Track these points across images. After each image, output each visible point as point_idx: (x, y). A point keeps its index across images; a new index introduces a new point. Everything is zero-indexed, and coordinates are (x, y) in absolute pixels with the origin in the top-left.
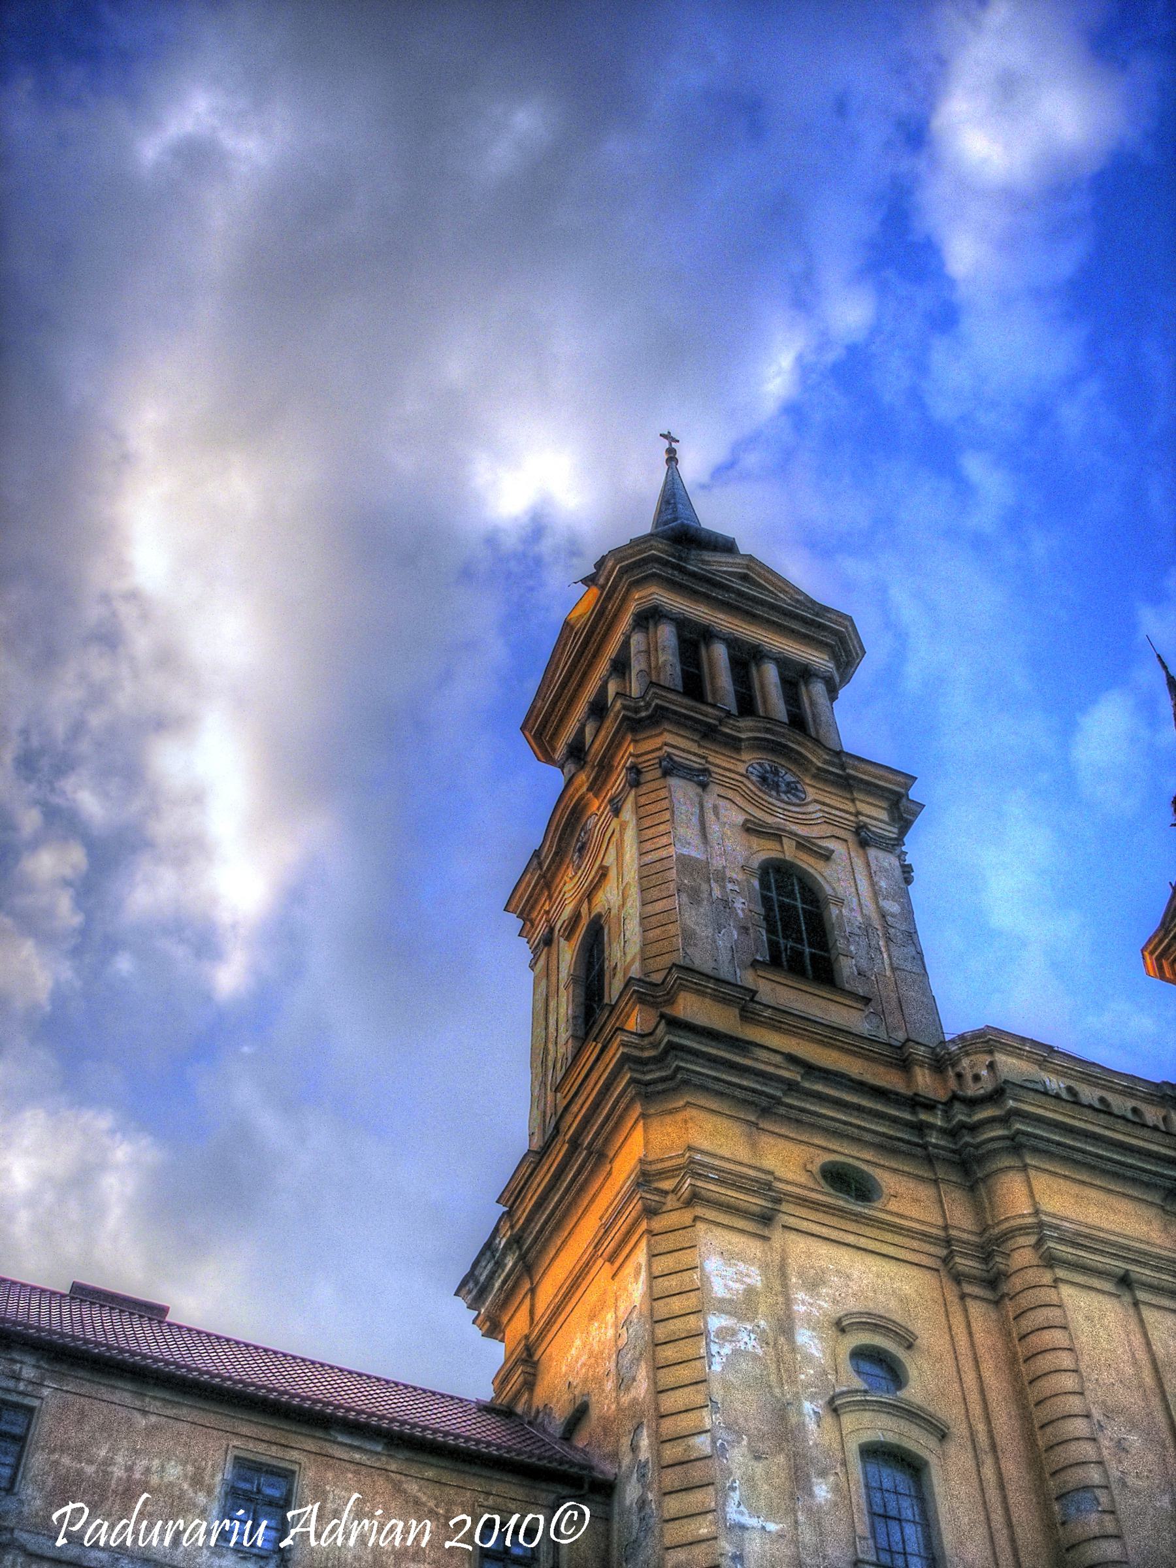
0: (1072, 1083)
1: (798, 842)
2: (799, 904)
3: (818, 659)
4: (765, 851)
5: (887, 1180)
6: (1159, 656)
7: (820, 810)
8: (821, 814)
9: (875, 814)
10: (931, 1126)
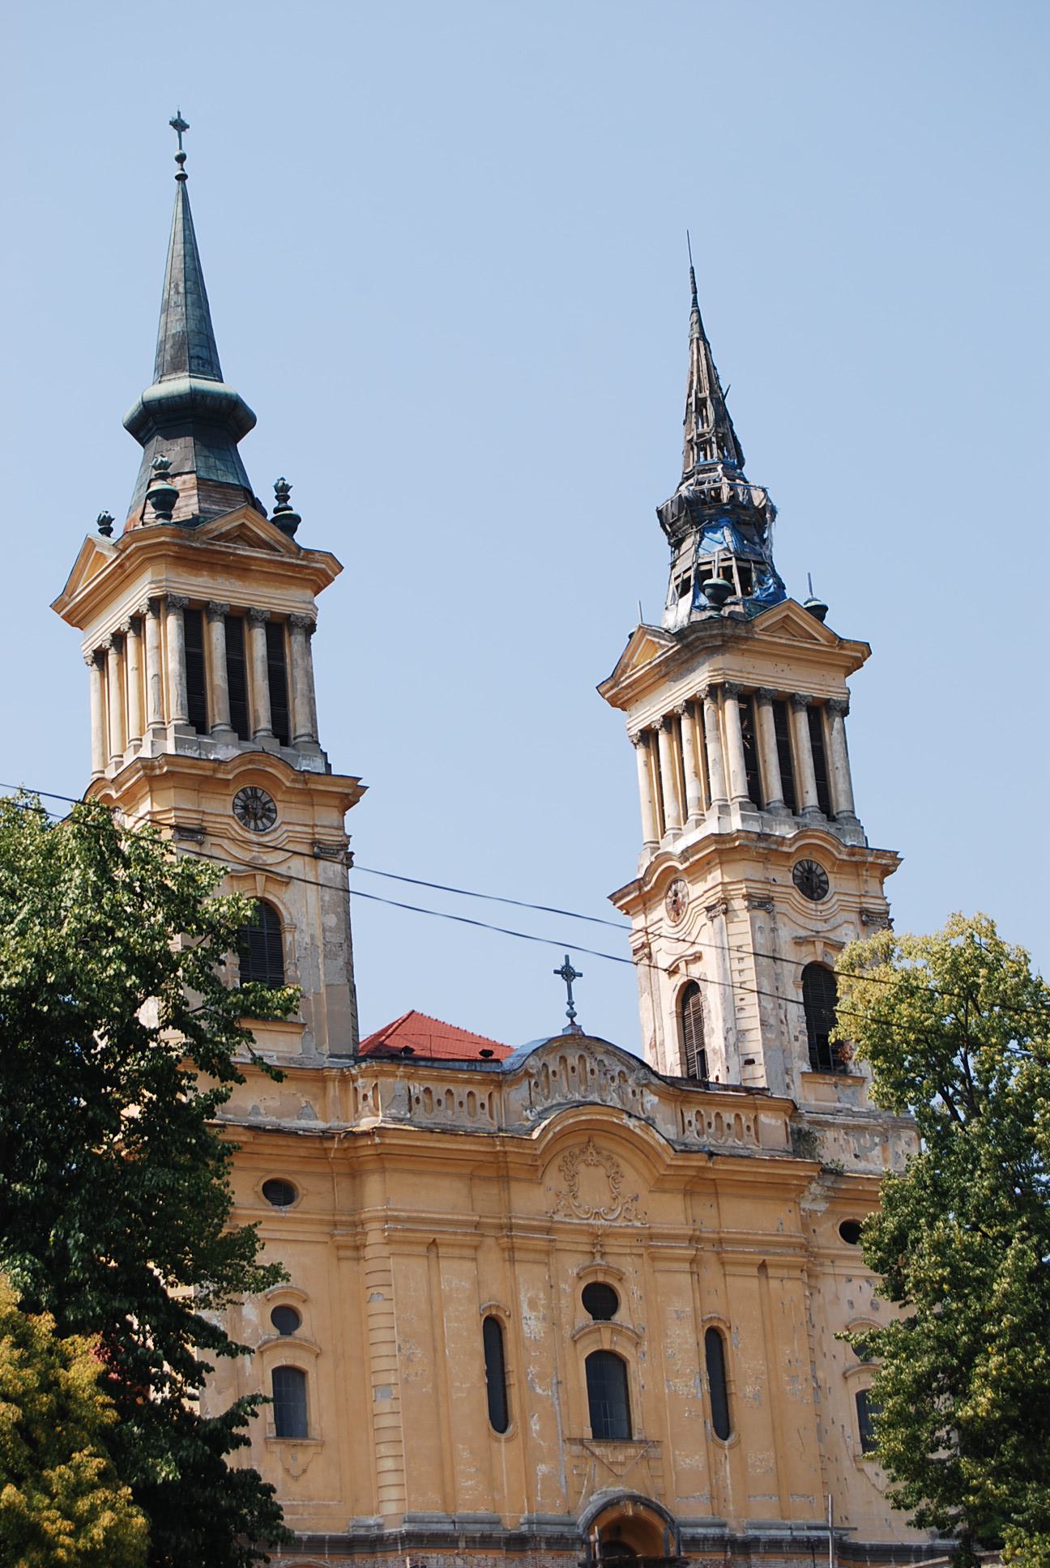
0: (428, 1085)
5: (302, 1183)
6: (692, 268)
8: (285, 835)
10: (331, 1149)
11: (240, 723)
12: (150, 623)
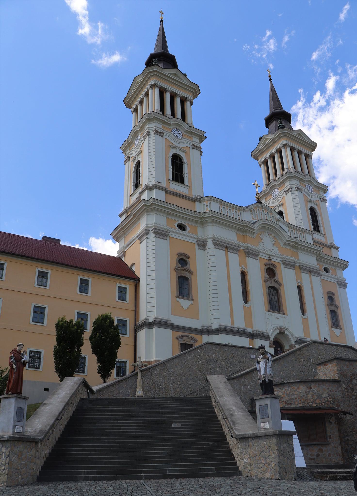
1: (180, 149)
2: (179, 162)
3: (189, 96)
4: (173, 151)
7: (185, 140)
9: (196, 140)
11: (173, 113)
12: (150, 91)
